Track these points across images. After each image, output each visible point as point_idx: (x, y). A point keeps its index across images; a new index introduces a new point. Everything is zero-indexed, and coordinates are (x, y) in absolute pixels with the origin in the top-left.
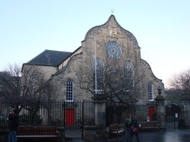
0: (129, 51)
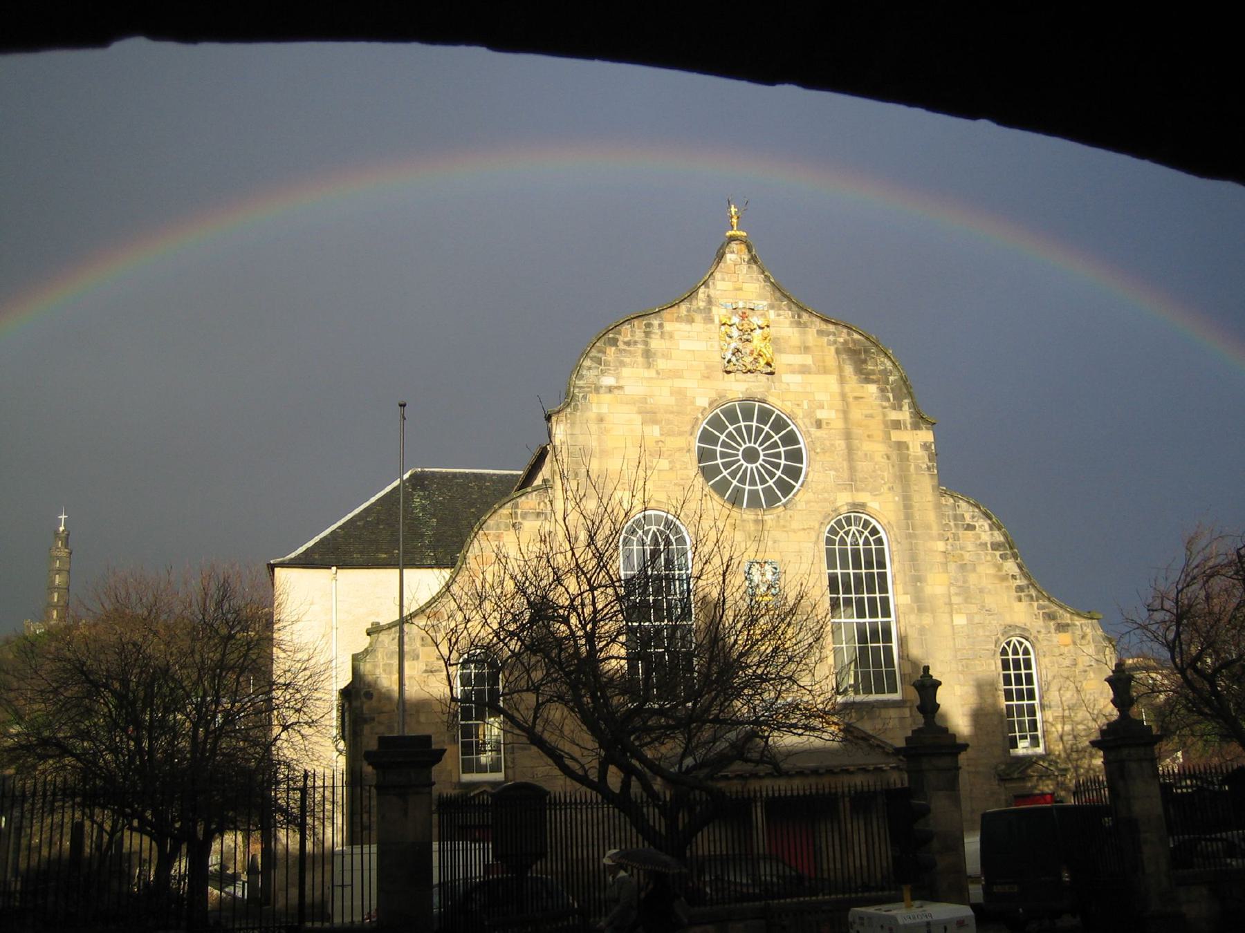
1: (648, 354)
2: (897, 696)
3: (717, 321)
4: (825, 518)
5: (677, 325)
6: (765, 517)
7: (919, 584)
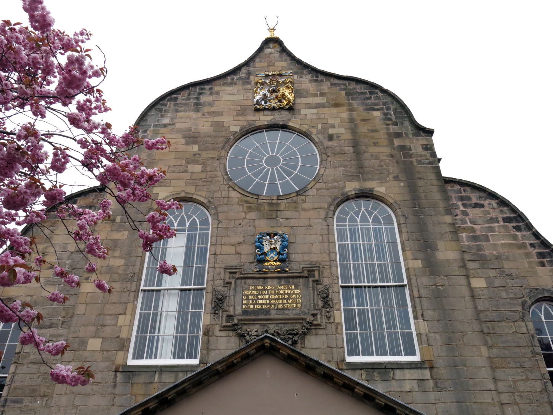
0: (358, 153)
1: (197, 104)
2: (416, 358)
3: (253, 83)
4: (334, 200)
5: (223, 88)
6: (279, 201)
7: (429, 251)
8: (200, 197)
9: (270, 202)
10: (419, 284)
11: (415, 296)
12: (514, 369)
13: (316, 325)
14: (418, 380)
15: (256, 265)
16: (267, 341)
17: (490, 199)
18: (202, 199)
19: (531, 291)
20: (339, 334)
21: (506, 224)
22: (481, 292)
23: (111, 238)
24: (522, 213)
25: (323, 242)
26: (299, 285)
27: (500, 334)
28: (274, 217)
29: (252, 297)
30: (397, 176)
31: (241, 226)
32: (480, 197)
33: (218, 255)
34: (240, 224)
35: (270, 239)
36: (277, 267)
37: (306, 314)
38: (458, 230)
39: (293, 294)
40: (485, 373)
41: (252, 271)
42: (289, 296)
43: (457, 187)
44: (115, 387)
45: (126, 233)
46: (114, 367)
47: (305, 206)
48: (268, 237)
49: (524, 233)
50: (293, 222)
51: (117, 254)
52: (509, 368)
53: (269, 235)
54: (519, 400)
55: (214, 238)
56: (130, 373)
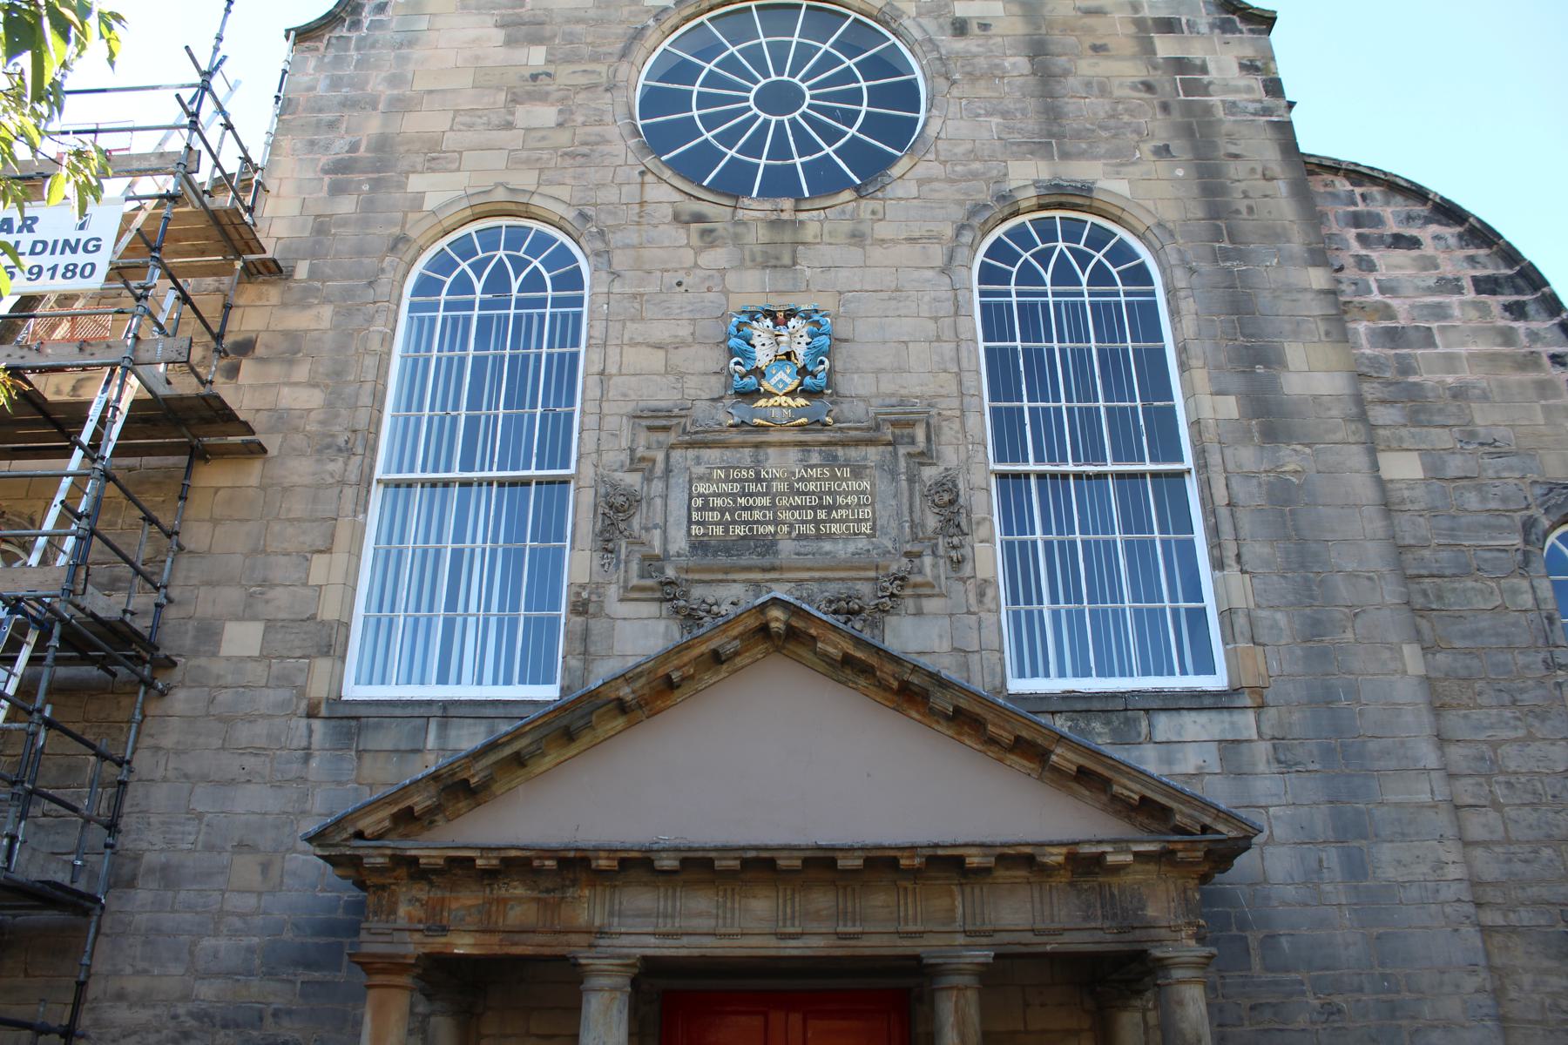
2: (1216, 682)
6: (802, 216)
7: (1260, 369)
8: (551, 201)
9: (774, 216)
10: (1231, 467)
11: (1216, 503)
12: (1494, 711)
13: (915, 586)
14: (1220, 741)
15: (733, 406)
16: (776, 613)
17: (1439, 223)
18: (559, 210)
19: (1551, 490)
20: (989, 611)
21: (1484, 297)
22: (1406, 493)
23: (279, 328)
24: (1531, 264)
25: (938, 339)
26: (865, 467)
27: (1457, 614)
28: (787, 260)
29: (719, 502)
30: (1166, 148)
31: (682, 289)
32: (1409, 218)
33: (611, 376)
34: (679, 284)
35: (774, 327)
36: (798, 412)
37: (889, 552)
38: (1345, 312)
39: (847, 494)
40: (1415, 725)
41: (720, 424)
42: (835, 500)
43: (1342, 185)
44: (307, 758)
45: (327, 311)
46: (303, 705)
47: (882, 230)
48: (768, 322)
49: (1534, 325)
50: (843, 278)
51: (302, 372)
52: (1481, 707)
53: (770, 314)
54: (1504, 796)
55: (600, 327)
56: (353, 723)
